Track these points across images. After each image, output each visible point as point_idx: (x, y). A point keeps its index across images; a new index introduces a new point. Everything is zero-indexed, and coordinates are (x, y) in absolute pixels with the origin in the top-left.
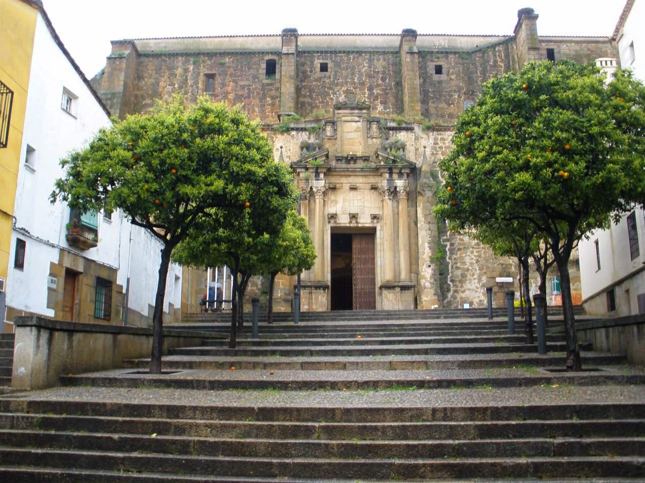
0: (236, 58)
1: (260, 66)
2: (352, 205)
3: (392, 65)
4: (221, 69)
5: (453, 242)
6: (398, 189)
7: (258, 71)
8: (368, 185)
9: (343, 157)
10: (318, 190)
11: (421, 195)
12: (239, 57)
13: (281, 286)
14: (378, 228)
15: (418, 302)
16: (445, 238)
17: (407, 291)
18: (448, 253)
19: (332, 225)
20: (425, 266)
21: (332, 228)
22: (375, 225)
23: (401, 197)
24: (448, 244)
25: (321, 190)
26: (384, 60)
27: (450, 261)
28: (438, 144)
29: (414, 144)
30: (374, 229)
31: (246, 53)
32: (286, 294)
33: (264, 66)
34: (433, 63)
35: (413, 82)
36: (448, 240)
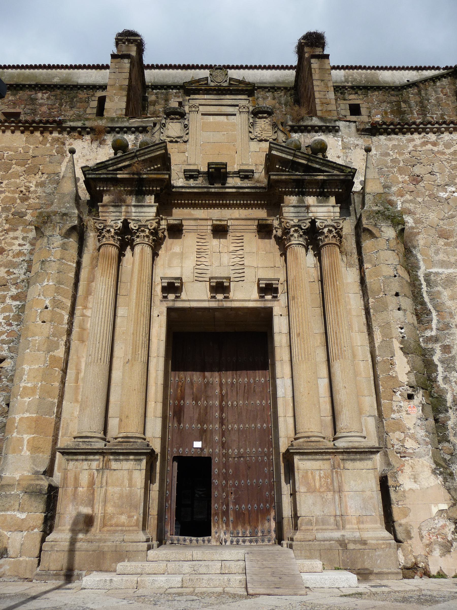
0: (53, 93)
1: (89, 105)
2: (216, 264)
3: (286, 105)
4: (30, 107)
5: (447, 342)
6: (318, 224)
7: (85, 111)
8: (249, 222)
9: (198, 171)
10: (140, 226)
11: (372, 235)
12: (58, 92)
13: (26, 452)
14: (277, 311)
15: (393, 496)
16: (428, 333)
17: (358, 464)
18: (440, 369)
19: (170, 304)
20: (398, 397)
21: (170, 310)
22: (269, 305)
23: (327, 241)
24: (437, 347)
25: (145, 226)
26: (274, 99)
27: (446, 386)
28: (388, 154)
29: (341, 154)
30: (268, 313)
31: (68, 86)
32: (36, 473)
33: (94, 104)
34: (345, 102)
35: (325, 95)
36: (436, 339)
